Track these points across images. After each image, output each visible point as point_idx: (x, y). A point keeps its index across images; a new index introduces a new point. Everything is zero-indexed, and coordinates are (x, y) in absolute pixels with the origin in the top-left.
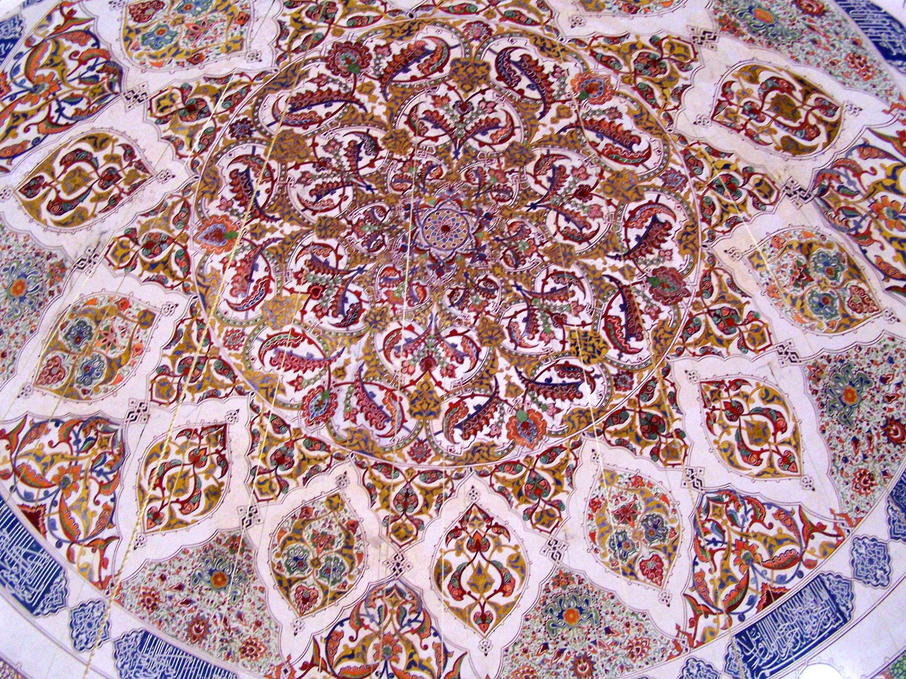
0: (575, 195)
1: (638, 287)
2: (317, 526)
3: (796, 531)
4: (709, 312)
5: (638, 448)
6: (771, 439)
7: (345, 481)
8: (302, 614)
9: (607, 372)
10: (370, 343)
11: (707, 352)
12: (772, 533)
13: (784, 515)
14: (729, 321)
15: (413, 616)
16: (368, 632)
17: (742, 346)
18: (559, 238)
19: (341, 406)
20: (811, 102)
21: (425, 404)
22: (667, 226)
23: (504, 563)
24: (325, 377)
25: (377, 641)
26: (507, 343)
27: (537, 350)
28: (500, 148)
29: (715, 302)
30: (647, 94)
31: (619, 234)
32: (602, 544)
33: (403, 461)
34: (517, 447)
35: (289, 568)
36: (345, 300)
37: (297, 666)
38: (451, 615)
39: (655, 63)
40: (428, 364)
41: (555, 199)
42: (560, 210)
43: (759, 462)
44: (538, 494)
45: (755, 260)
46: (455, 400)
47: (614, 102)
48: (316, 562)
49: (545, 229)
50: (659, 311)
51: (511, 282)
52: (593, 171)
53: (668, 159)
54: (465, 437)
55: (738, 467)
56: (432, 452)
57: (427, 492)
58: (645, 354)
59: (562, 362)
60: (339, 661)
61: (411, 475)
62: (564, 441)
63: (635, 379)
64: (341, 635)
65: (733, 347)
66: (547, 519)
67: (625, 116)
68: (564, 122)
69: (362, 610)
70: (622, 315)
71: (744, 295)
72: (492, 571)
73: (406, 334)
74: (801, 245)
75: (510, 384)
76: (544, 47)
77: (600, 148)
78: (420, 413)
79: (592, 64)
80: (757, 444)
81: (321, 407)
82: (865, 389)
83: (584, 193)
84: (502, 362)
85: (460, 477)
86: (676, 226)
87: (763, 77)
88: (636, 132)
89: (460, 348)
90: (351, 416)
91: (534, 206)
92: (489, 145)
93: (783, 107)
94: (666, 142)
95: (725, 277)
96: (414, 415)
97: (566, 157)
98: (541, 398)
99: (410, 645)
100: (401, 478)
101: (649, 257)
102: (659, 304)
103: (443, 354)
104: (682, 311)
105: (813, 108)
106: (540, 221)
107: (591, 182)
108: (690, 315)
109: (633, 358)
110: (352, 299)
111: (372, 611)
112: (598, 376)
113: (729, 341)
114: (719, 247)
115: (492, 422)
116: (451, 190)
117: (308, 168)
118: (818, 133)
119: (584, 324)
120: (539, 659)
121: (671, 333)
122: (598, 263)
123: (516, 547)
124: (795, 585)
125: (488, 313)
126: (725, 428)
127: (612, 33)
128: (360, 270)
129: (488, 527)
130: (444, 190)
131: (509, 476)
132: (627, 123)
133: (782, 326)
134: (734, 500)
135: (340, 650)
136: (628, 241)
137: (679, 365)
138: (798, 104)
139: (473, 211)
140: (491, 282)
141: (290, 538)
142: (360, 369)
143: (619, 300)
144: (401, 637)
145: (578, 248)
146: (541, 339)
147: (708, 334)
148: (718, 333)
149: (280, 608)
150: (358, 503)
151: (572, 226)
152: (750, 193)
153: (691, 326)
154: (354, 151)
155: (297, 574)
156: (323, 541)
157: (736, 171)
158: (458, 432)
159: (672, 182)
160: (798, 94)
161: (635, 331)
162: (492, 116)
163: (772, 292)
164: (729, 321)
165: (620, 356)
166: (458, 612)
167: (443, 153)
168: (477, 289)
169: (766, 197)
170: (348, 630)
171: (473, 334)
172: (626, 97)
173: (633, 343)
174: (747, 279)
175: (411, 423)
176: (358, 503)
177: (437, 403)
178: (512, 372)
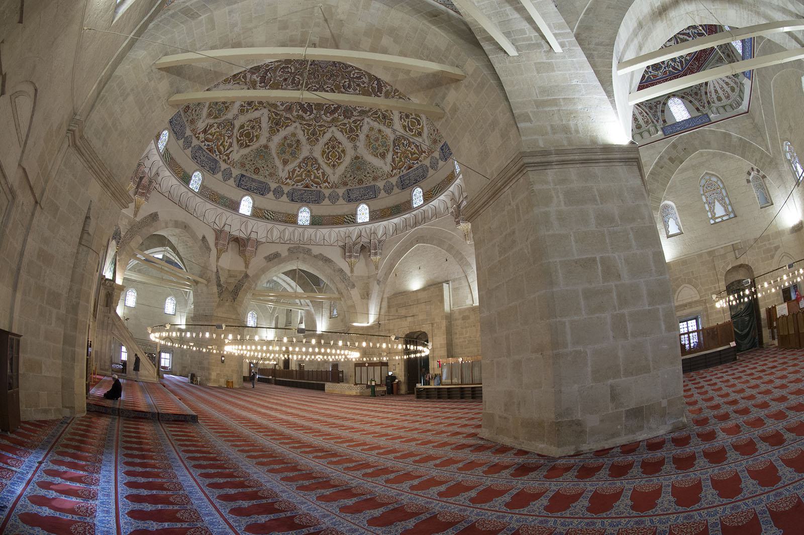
18: (290, 66)
30: (277, 114)
39: (277, 124)
42: (291, 73)
47: (283, 108)
49: (294, 66)
76: (302, 118)
83: (285, 80)
86: (259, 84)
95: (241, 83)
106: (296, 69)
116: (323, 71)
117: (362, 85)
127: (288, 128)
154: (349, 87)
167: (326, 83)
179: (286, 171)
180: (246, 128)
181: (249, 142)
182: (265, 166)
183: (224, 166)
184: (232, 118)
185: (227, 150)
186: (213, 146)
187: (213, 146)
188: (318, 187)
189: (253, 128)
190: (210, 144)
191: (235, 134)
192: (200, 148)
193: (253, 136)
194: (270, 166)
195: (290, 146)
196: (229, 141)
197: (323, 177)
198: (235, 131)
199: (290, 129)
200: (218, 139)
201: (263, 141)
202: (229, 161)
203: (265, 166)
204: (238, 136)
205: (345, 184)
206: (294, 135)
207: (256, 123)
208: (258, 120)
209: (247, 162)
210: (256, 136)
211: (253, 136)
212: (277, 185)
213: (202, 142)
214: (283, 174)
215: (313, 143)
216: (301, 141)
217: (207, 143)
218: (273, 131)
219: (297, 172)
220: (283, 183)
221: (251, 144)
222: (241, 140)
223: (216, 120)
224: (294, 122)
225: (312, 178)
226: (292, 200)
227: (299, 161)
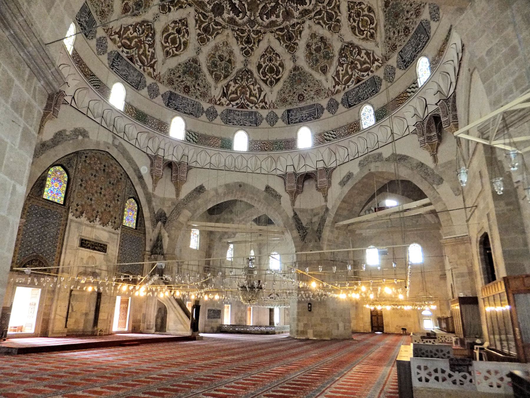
3: (151, 61)
4: (209, 24)
6: (173, 46)
11: (196, 21)
12: (147, 52)
13: (153, 55)
17: (199, 35)
22: (238, 16)
29: (212, 25)
43: (166, 42)
53: (259, 25)
55: (163, 34)
65: (198, 31)
71: (215, 37)
76: (306, 12)
79: (295, 20)
80: (171, 41)
82: (194, 79)
88: (270, 20)
94: (264, 27)
101: (228, 6)
102: (212, 5)
108: (208, 16)
113: (200, 30)
114: (229, 31)
124: (137, 67)
126: (173, 28)
127: (303, 34)
132: (273, 18)
133: (207, 49)
134: (152, 35)
148: (203, 26)
152: (246, 48)
157: (253, 46)
159: (252, 23)
163: (216, 48)
164: (206, 30)
172: (282, 23)
174: (220, 39)
179: (330, 78)
180: (264, 65)
181: (277, 76)
182: (307, 88)
183: (264, 113)
184: (243, 66)
185: (260, 96)
186: (243, 101)
187: (243, 101)
188: (370, 73)
189: (270, 60)
190: (238, 101)
191: (258, 78)
192: (230, 111)
193: (277, 68)
194: (311, 84)
195: (318, 50)
196: (256, 88)
197: (369, 58)
198: (256, 75)
199: (306, 33)
200: (244, 93)
201: (289, 65)
202: (268, 106)
203: (307, 88)
204: (262, 78)
205: (394, 48)
206: (313, 36)
207: (270, 54)
208: (270, 50)
209: (286, 96)
210: (280, 65)
211: (277, 68)
212: (328, 99)
213: (228, 105)
214: (327, 83)
215: (337, 28)
216: (325, 35)
218: (291, 49)
219: (341, 72)
220: (333, 94)
221: (280, 76)
222: (267, 79)
223: (229, 79)
224: (304, 22)
225: (359, 67)
226: (350, 106)
227: (336, 59)
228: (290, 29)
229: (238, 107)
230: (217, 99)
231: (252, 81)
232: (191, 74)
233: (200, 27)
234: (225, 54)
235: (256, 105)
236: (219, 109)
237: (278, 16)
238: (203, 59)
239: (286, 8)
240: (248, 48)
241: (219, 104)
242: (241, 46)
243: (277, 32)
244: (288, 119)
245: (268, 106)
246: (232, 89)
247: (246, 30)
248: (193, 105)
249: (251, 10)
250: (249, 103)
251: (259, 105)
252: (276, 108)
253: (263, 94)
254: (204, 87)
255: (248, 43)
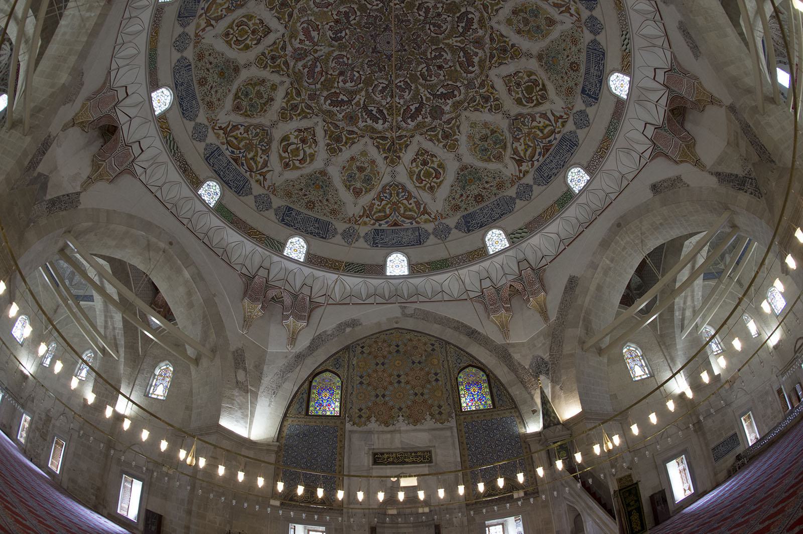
0: (437, 66)
1: (427, 106)
2: (262, 89)
5: (382, 152)
7: (282, 84)
8: (233, 111)
9: (392, 123)
10: (333, 52)
11: (431, 140)
14: (446, 136)
15: (265, 145)
16: (247, 136)
17: (445, 146)
19: (305, 61)
20: (540, 93)
21: (328, 84)
23: (308, 153)
24: (310, 48)
25: (248, 142)
26: (370, 89)
27: (377, 99)
28: (433, 34)
29: (447, 128)
30: (492, 56)
31: (437, 87)
32: (345, 172)
33: (304, 95)
34: (343, 122)
35: (242, 93)
36: (341, 32)
37: (218, 125)
38: (277, 155)
39: (505, 51)
40: (341, 73)
41: (430, 62)
42: (428, 66)
44: (336, 142)
45: (473, 125)
46: (338, 91)
48: (251, 99)
49: (417, 67)
50: (427, 118)
51: (391, 73)
52: (450, 64)
54: (330, 105)
56: (316, 101)
57: (302, 110)
58: (410, 127)
59: (381, 109)
60: (231, 136)
61: (303, 101)
62: (359, 132)
63: (399, 132)
64: (239, 129)
66: (333, 151)
67: (478, 57)
68: (459, 44)
69: (251, 128)
70: (413, 110)
71: (459, 132)
72: (302, 153)
73: (345, 59)
74: (493, 130)
75: (359, 102)
77: (459, 60)
78: (324, 85)
79: (487, 37)
81: (300, 55)
83: (440, 67)
84: (363, 93)
85: (317, 115)
86: (457, 98)
87: (533, 77)
89: (355, 78)
90: (304, 66)
91: (422, 58)
92: (431, 31)
93: (529, 90)
94: (481, 73)
96: (321, 84)
97: (447, 54)
98: (364, 114)
99: (257, 152)
100: (299, 99)
103: (349, 75)
104: (434, 123)
105: (539, 95)
107: (446, 66)
109: (405, 125)
110: (343, 34)
111: (254, 131)
112: (388, 122)
113: (441, 142)
115: (342, 107)
118: (532, 103)
119: (399, 103)
120: (297, 192)
121: (424, 127)
122: (422, 90)
123: (315, 152)
125: (374, 75)
128: (355, 29)
129: (312, 138)
130: (402, 31)
131: (332, 128)
132: (476, 60)
135: (234, 134)
136: (438, 91)
137: (418, 138)
138: (535, 91)
139: (402, 45)
140: (385, 68)
141: (251, 84)
142: (322, 56)
143: (417, 105)
144: (256, 148)
145: (421, 81)
146: (382, 97)
147: (436, 135)
148: (440, 137)
149: (229, 102)
150: (280, 94)
151: (426, 73)
152: (491, 106)
153: (433, 129)
155: (243, 97)
156: (259, 95)
157: (494, 97)
158: (329, 101)
160: (538, 88)
161: (413, 118)
162: (442, 25)
163: (471, 137)
164: (446, 136)
165: (401, 121)
166: (280, 155)
167: (417, 21)
168: (379, 66)
169: (495, 110)
170: (242, 130)
171: (363, 77)
172: (485, 52)
173: (409, 121)
174: (465, 128)
175: (318, 86)
176: (280, 94)
177: (332, 87)
178: (363, 99)
184: (507, 121)
186: (542, 145)
187: (542, 145)
190: (538, 151)
192: (539, 169)
196: (538, 119)
198: (525, 111)
200: (535, 137)
202: (565, 116)
204: (532, 105)
207: (512, 81)
208: (507, 79)
213: (533, 165)
217: (536, 157)
218: (516, 53)
221: (540, 82)
222: (537, 99)
228: (495, 46)
229: (543, 156)
230: (518, 174)
231: (528, 119)
232: (471, 182)
233: (438, 140)
234: (484, 132)
235: (556, 131)
236: (528, 179)
237: (476, 54)
238: (469, 159)
239: (471, 42)
240: (492, 103)
241: (524, 175)
242: (486, 110)
243: (493, 62)
244: (592, 97)
245: (565, 116)
246: (521, 149)
247: (473, 95)
248: (498, 204)
249: (456, 79)
250: (549, 139)
251: (559, 128)
252: (573, 106)
253: (549, 115)
254: (494, 178)
255: (489, 101)
